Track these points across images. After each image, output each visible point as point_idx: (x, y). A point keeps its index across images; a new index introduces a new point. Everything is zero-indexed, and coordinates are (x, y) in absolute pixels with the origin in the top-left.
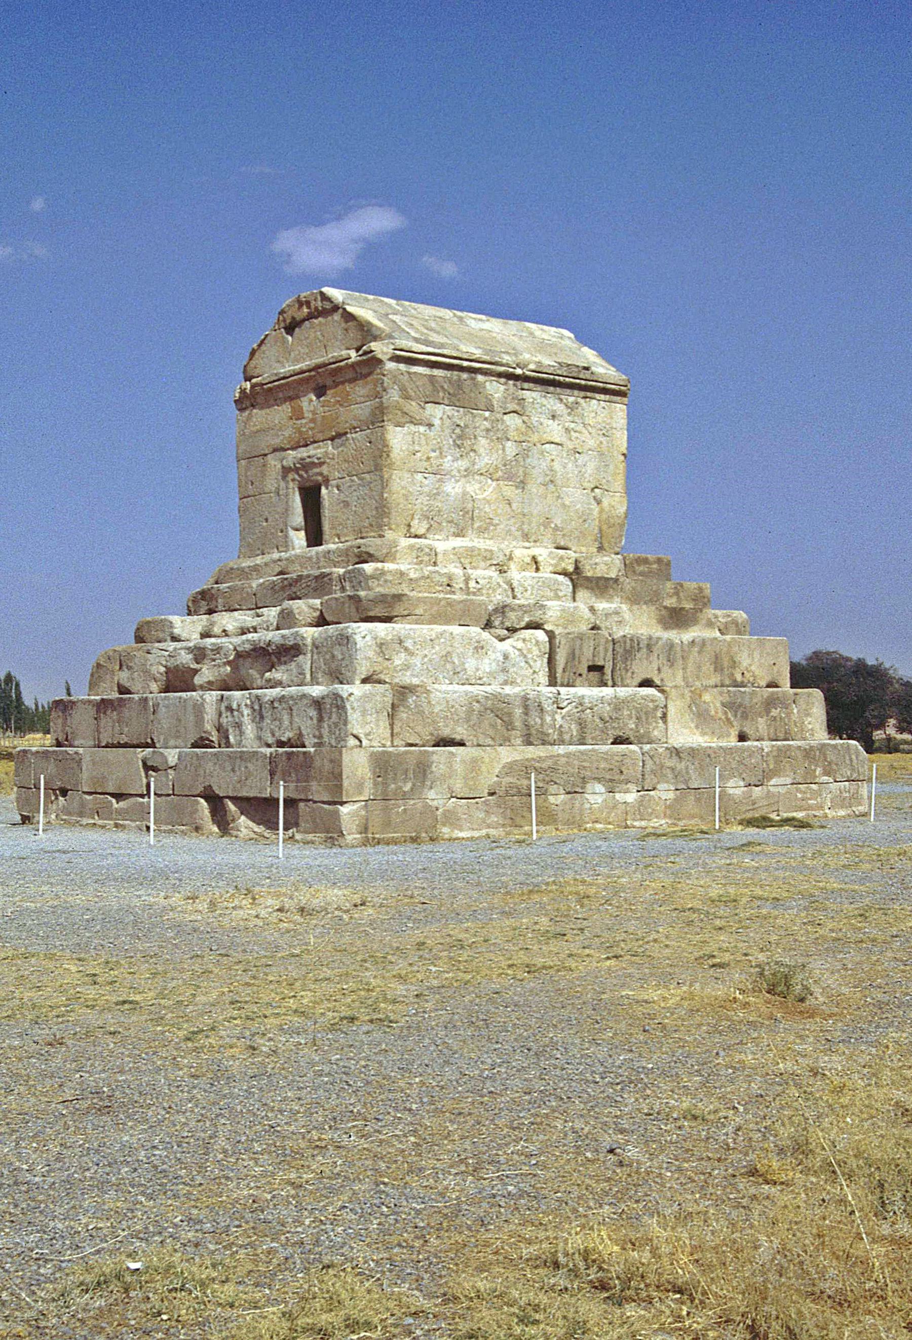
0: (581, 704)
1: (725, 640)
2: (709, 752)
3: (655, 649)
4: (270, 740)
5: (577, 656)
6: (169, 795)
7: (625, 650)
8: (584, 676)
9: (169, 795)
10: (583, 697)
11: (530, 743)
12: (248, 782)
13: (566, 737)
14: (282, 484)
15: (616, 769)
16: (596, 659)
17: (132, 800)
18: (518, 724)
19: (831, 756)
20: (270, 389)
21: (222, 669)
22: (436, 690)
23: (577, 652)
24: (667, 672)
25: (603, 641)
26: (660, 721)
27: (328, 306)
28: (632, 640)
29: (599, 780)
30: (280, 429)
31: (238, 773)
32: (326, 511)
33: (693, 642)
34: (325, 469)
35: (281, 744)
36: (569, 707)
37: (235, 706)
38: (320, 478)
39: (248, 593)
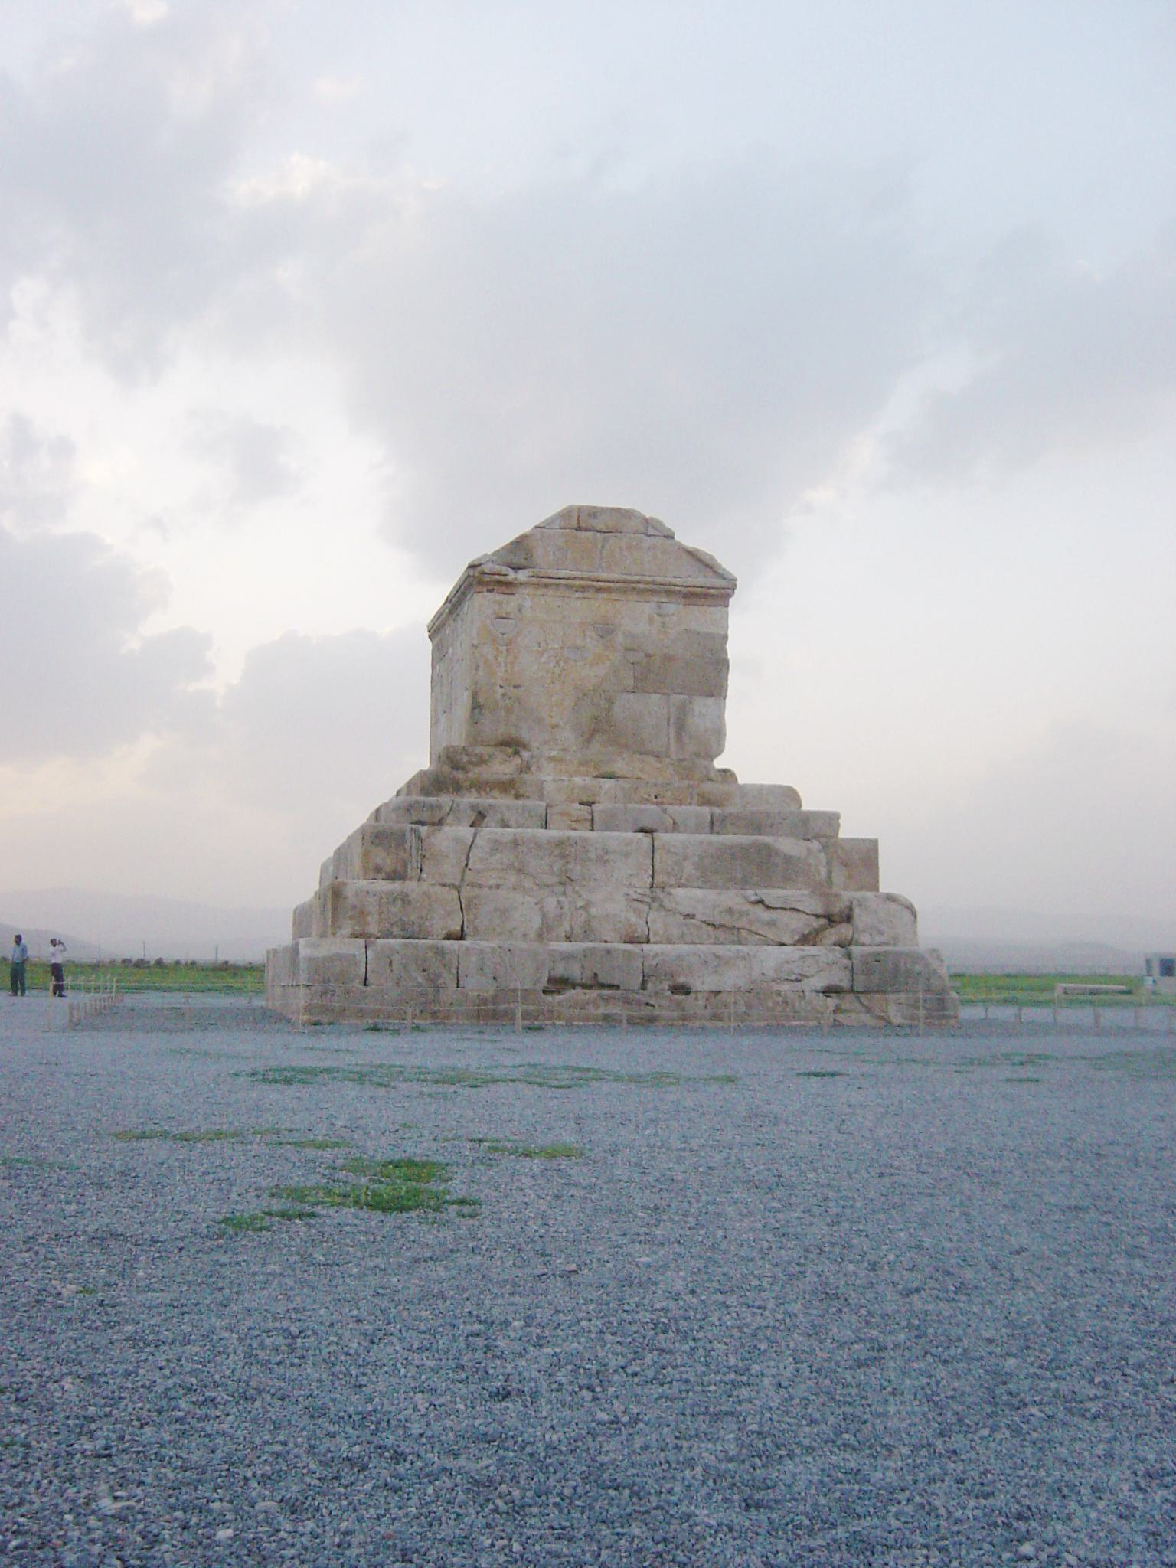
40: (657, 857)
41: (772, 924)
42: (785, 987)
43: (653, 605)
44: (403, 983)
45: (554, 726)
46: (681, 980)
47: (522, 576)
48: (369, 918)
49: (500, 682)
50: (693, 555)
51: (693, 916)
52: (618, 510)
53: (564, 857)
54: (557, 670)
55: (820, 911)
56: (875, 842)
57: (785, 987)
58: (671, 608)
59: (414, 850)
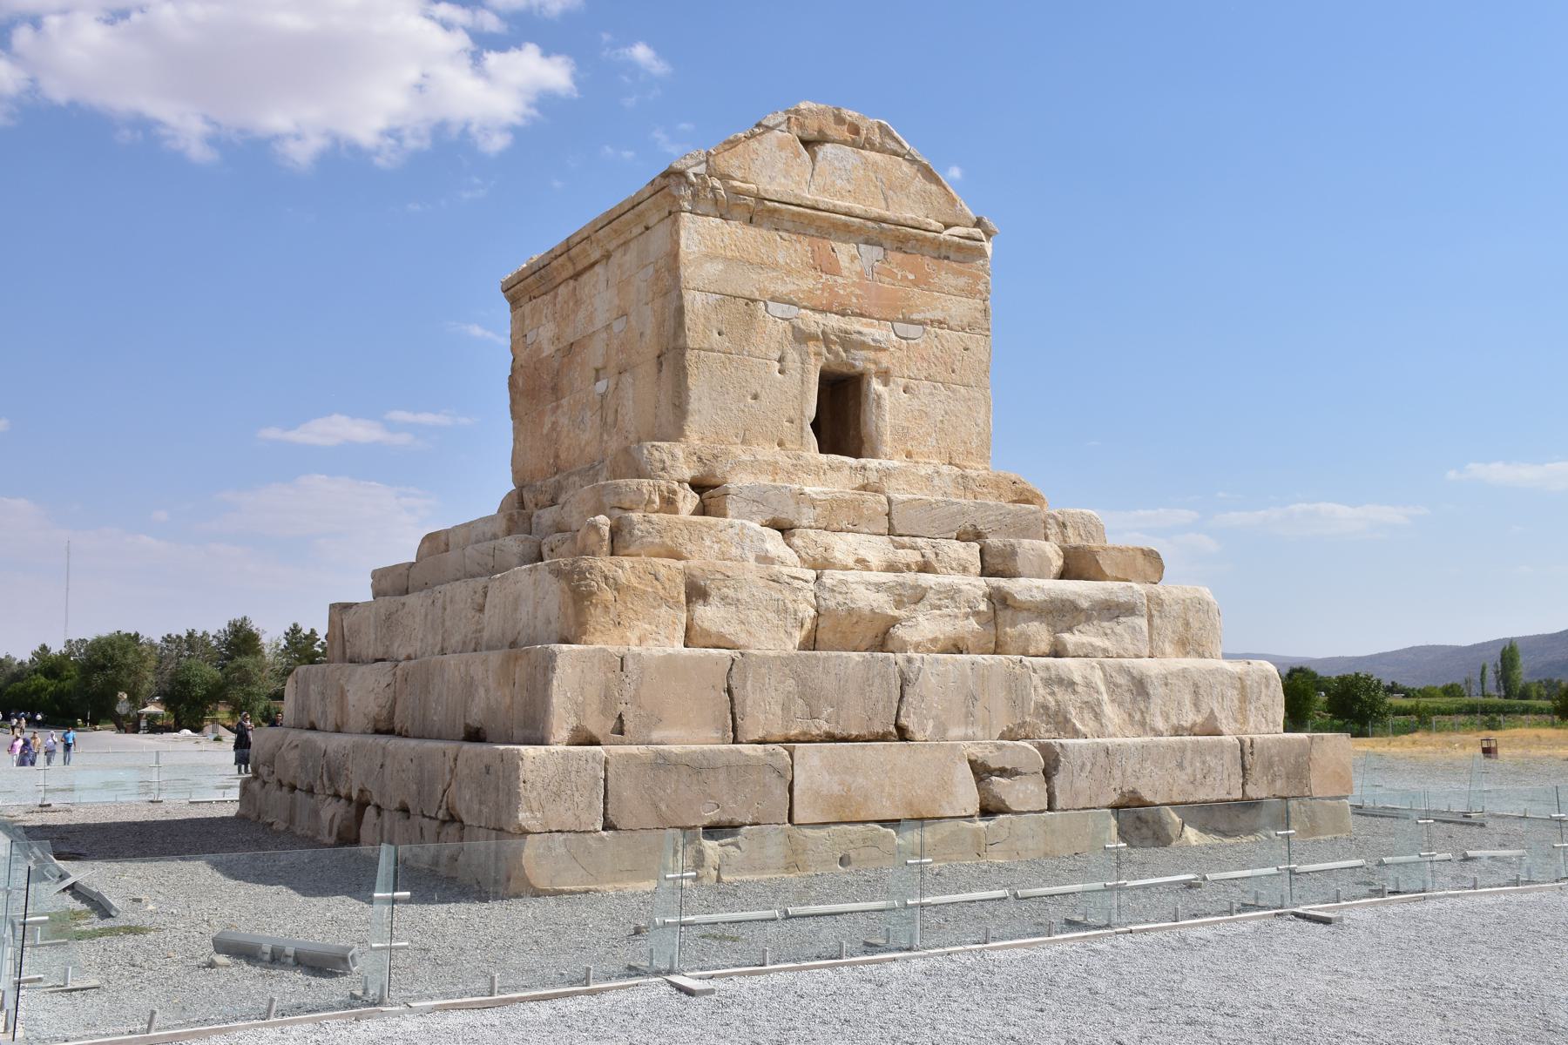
4: (1160, 724)
6: (1041, 811)
9: (1041, 811)
12: (1209, 780)
14: (793, 356)
17: (948, 826)
20: (775, 210)
21: (960, 623)
27: (892, 145)
30: (789, 273)
31: (1189, 770)
32: (887, 417)
34: (885, 360)
35: (1177, 731)
37: (1077, 678)
38: (872, 367)
39: (875, 510)
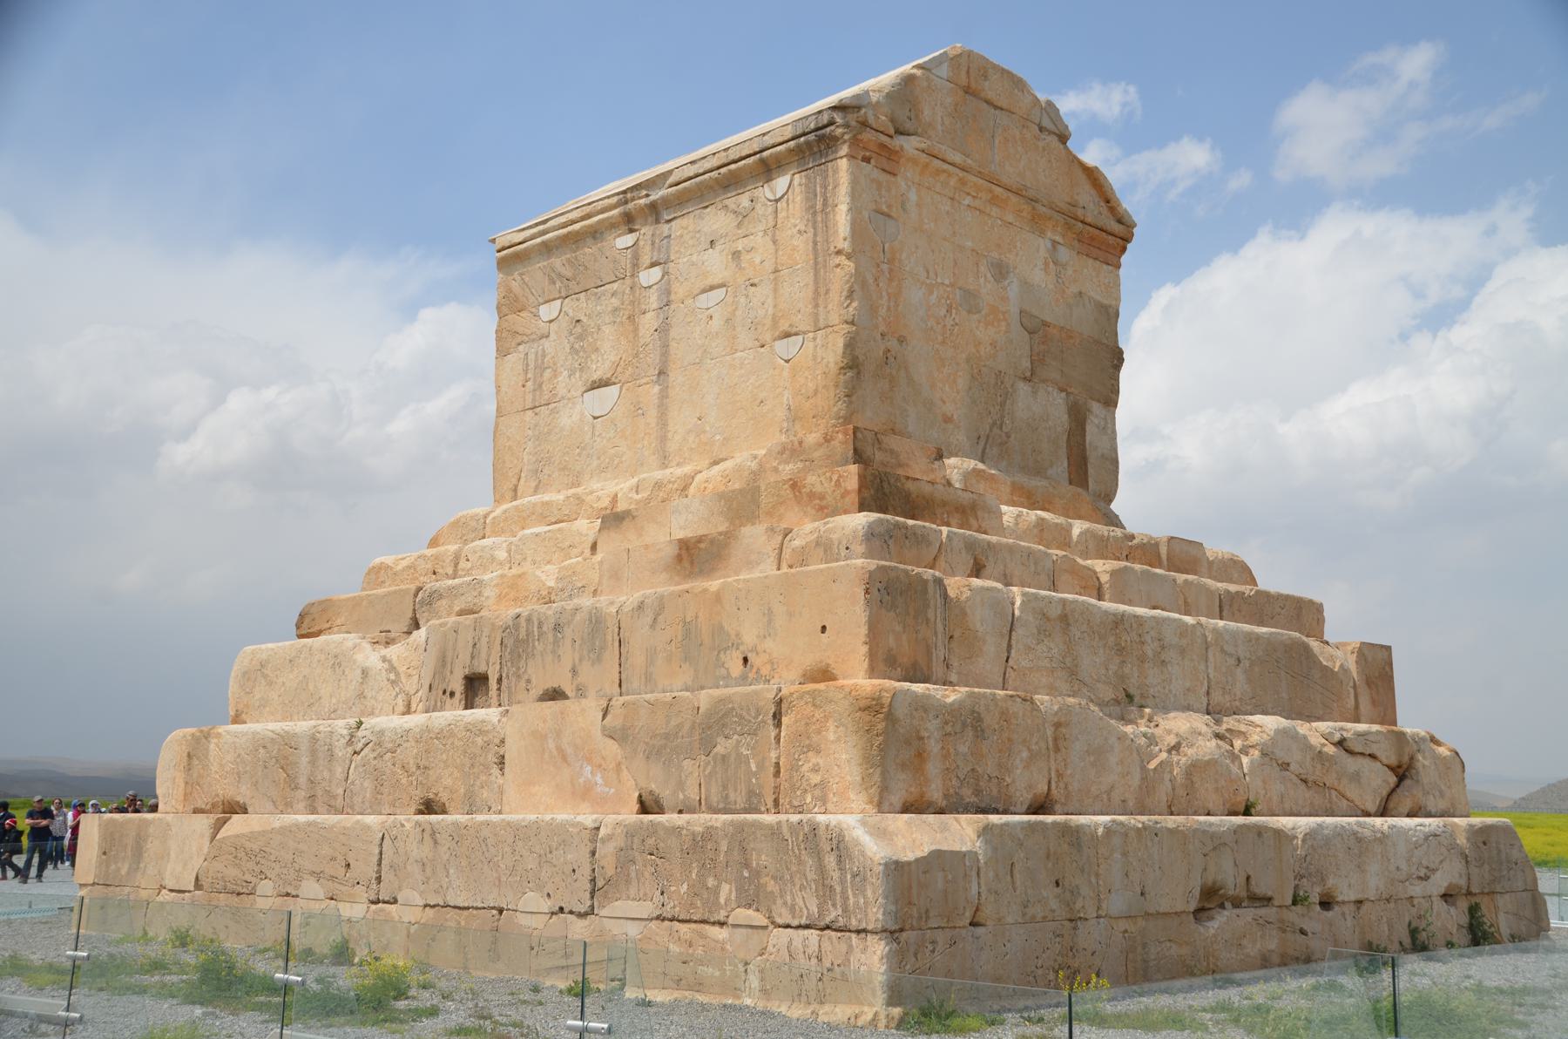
0: (380, 744)
1: (705, 590)
2: (486, 832)
3: (568, 631)
5: (449, 660)
7: (517, 641)
8: (458, 695)
10: (382, 732)
11: (314, 811)
13: (357, 800)
15: (340, 858)
16: (476, 662)
18: (302, 780)
19: (763, 857)
22: (228, 732)
23: (449, 654)
24: (587, 674)
25: (486, 632)
26: (495, 770)
28: (529, 620)
29: (318, 876)
33: (641, 606)
36: (366, 750)
40: (1211, 658)
41: (1356, 777)
42: (1417, 889)
43: (1049, 245)
44: (1031, 911)
45: (948, 419)
46: (1331, 882)
47: (909, 145)
48: (933, 768)
49: (882, 328)
50: (1093, 177)
51: (1285, 766)
52: (1009, 72)
53: (1121, 650)
54: (949, 322)
55: (1393, 761)
56: (1388, 648)
57: (1417, 889)
58: (1064, 254)
59: (940, 627)
